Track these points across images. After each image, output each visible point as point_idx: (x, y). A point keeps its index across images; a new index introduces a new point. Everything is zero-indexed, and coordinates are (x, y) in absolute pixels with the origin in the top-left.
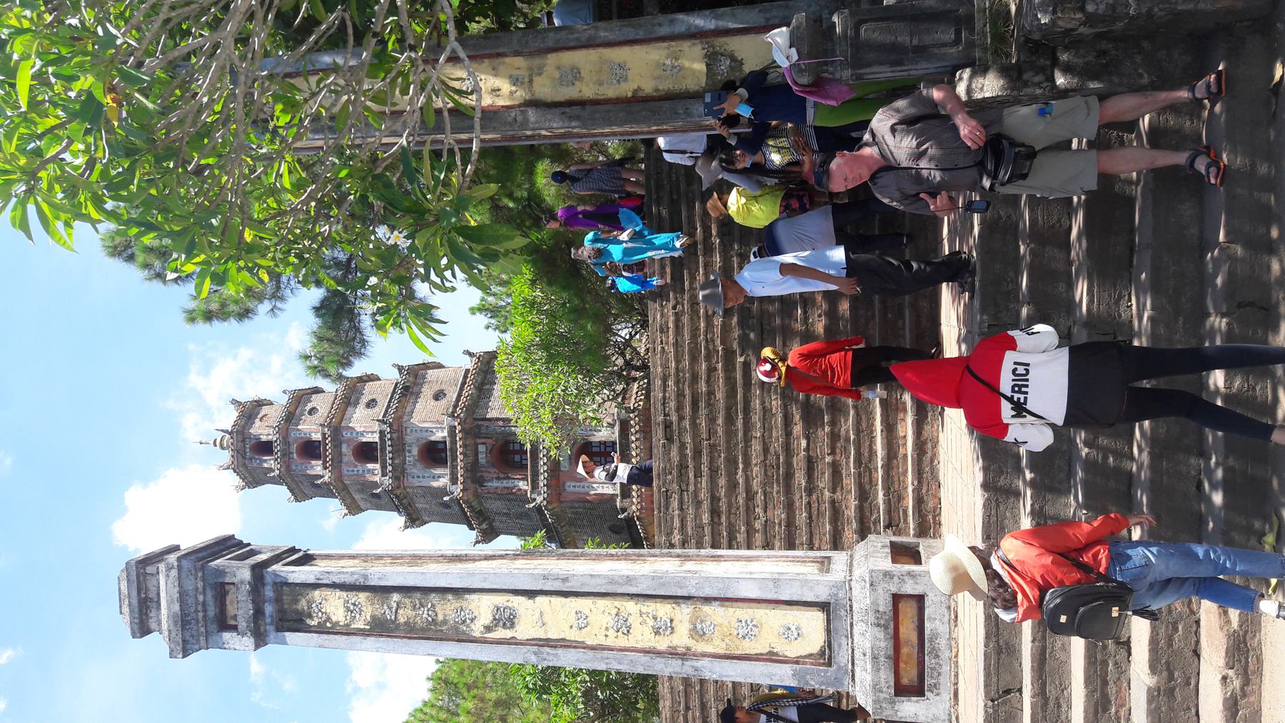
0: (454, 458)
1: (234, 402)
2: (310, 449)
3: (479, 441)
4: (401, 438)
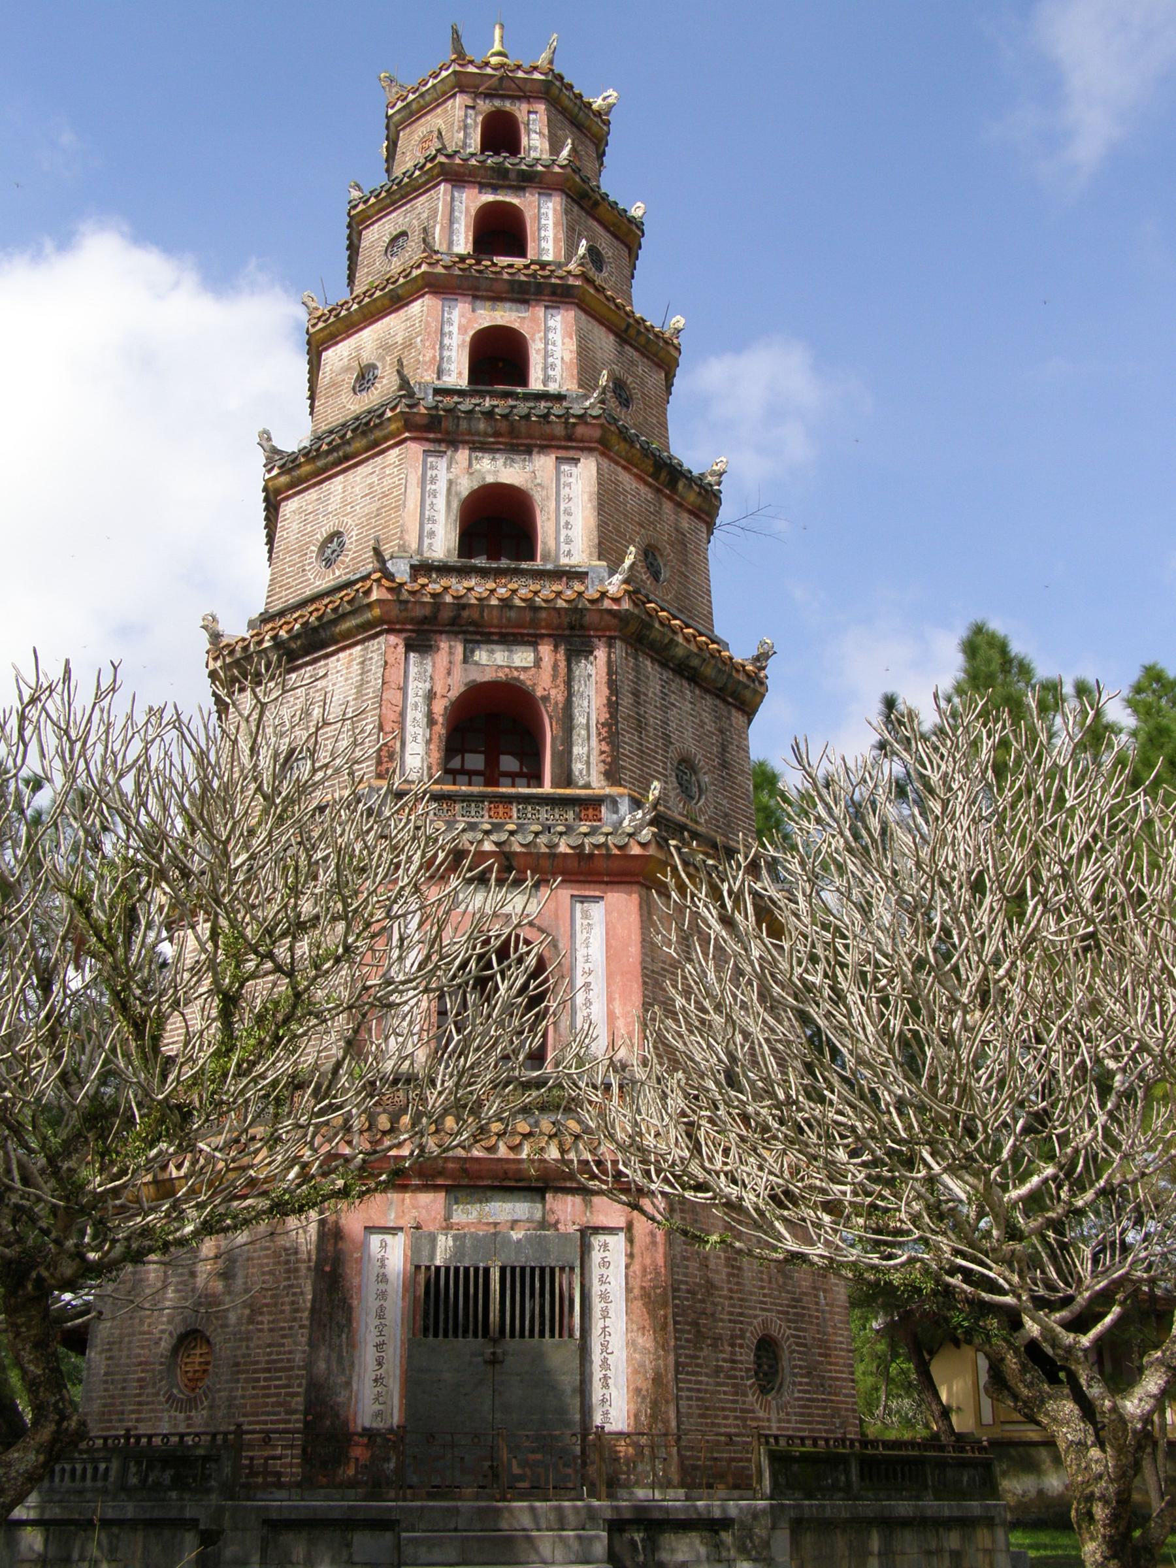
2: (500, 231)
3: (545, 650)
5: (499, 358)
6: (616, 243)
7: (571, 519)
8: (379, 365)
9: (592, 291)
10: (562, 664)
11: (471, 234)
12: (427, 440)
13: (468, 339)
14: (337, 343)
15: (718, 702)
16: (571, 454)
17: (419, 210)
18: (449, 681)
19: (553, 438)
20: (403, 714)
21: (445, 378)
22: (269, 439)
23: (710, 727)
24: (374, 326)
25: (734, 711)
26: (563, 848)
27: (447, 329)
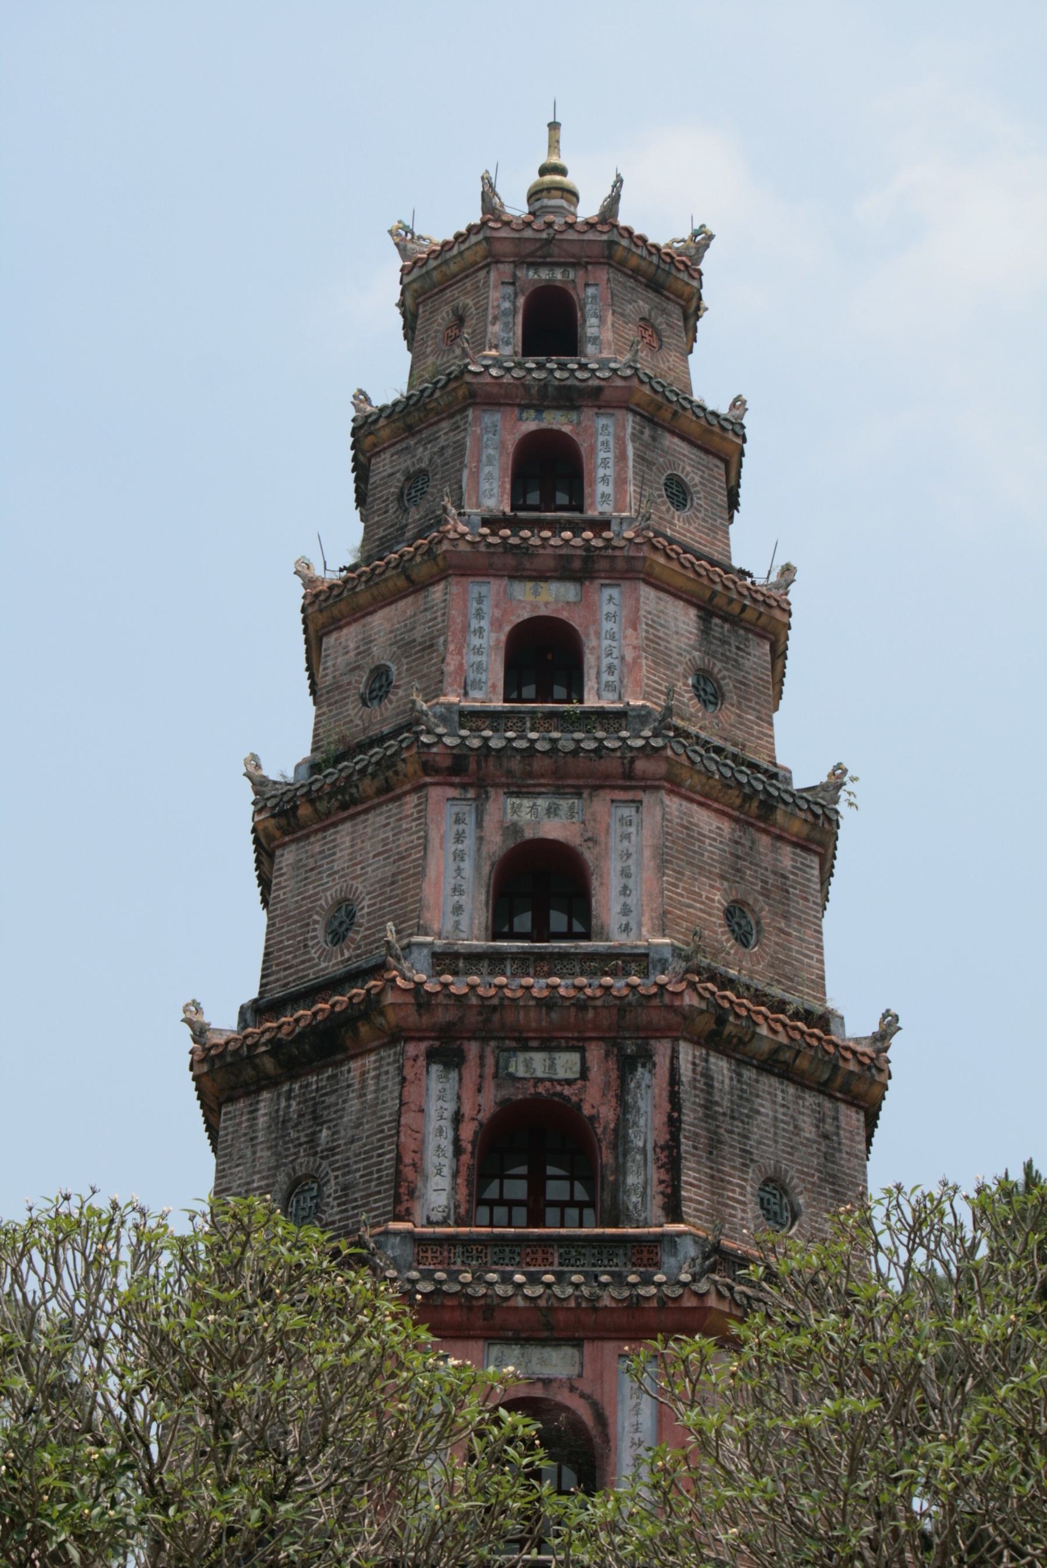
0: (525, 962)
1: (701, 240)
2: (549, 471)
3: (595, 1053)
4: (599, 784)
5: (545, 657)
7: (631, 883)
8: (394, 668)
9: (662, 560)
10: (614, 1074)
11: (508, 480)
12: (452, 785)
13: (503, 638)
14: (340, 628)
15: (821, 1098)
16: (630, 795)
17: (442, 442)
18: (481, 1099)
19: (607, 777)
20: (423, 1141)
21: (474, 694)
22: (258, 766)
23: (809, 1131)
25: (842, 1107)
26: (606, 1302)
27: (474, 624)
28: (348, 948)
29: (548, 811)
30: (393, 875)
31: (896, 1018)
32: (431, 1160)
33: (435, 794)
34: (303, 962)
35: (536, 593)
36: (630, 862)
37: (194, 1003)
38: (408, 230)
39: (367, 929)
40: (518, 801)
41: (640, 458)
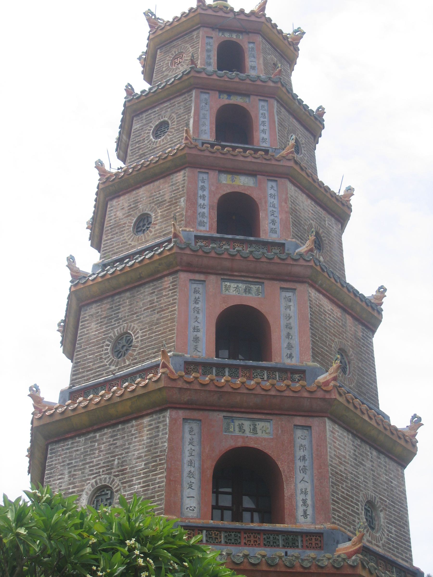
1: (299, 34)
6: (307, 133)
7: (291, 332)
8: (153, 215)
13: (216, 201)
24: (148, 187)
27: (200, 193)
28: (129, 360)
29: (245, 291)
30: (157, 319)
31: (420, 419)
32: (186, 480)
33: (183, 276)
34: (99, 367)
35: (233, 180)
36: (291, 321)
37: (36, 386)
38: (153, 14)
39: (140, 349)
40: (228, 284)
41: (280, 124)
